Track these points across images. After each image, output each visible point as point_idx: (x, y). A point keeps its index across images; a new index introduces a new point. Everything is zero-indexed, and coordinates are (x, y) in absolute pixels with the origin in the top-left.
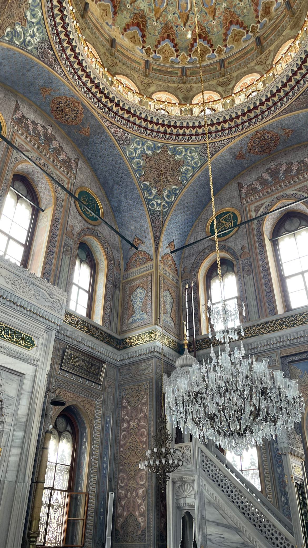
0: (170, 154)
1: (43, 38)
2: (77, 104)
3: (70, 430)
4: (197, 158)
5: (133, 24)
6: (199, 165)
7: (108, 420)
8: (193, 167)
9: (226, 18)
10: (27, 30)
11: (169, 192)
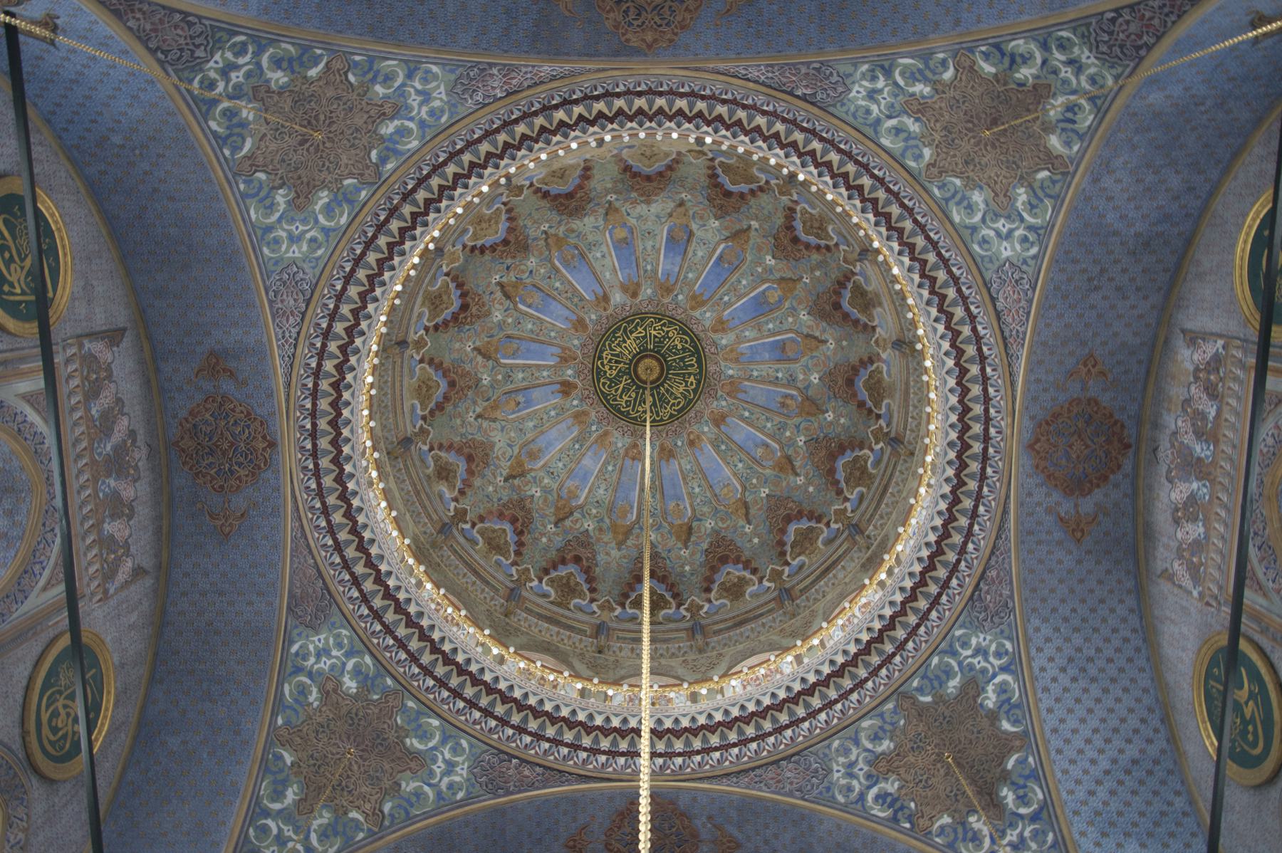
0: (346, 182)
1: (843, 105)
2: (649, 37)
4: (287, 251)
5: (580, 187)
6: (266, 250)
8: (269, 229)
9: (465, 374)
10: (896, 96)
11: (243, 124)
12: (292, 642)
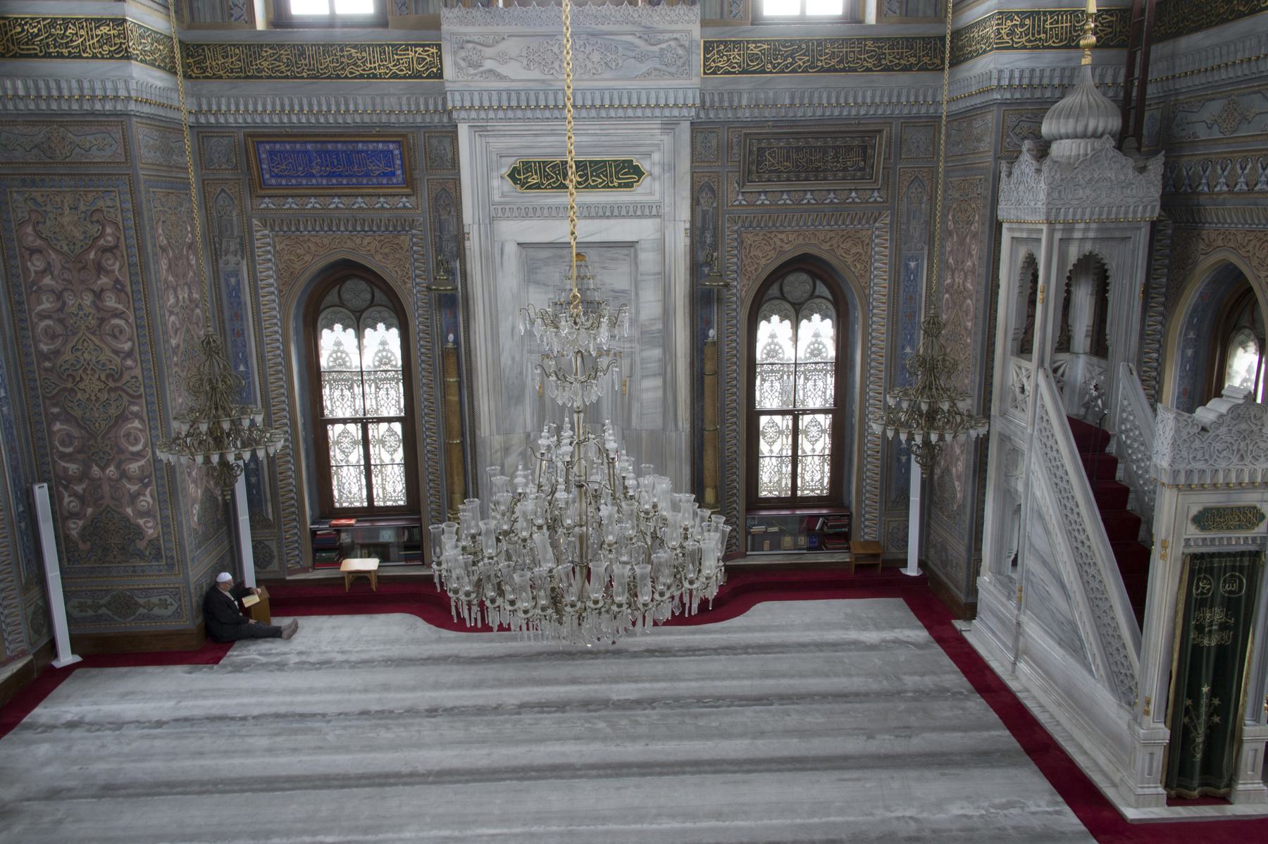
3: (827, 294)
7: (913, 264)
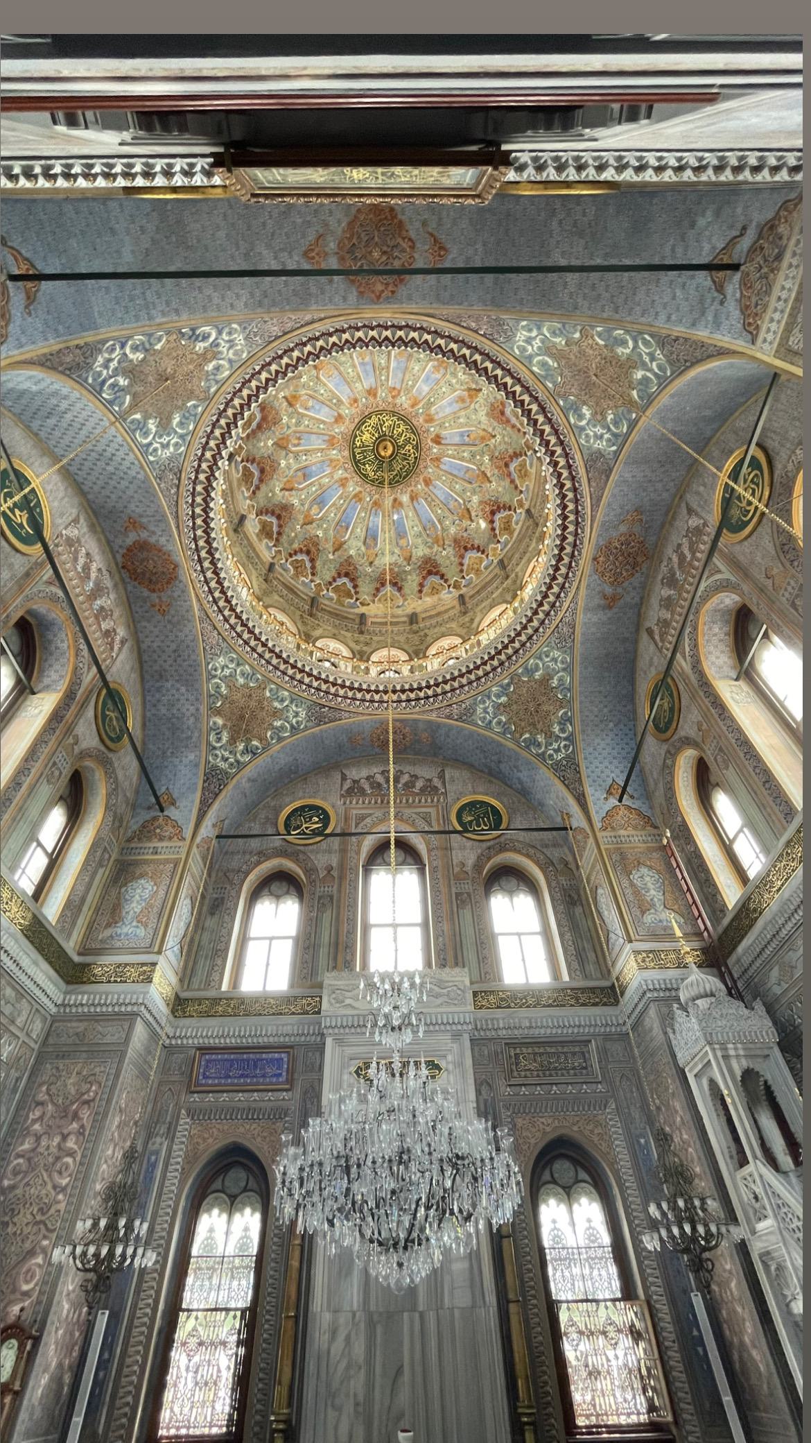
3: (587, 1178)
7: (642, 1141)
11: (560, 723)
12: (615, 452)
